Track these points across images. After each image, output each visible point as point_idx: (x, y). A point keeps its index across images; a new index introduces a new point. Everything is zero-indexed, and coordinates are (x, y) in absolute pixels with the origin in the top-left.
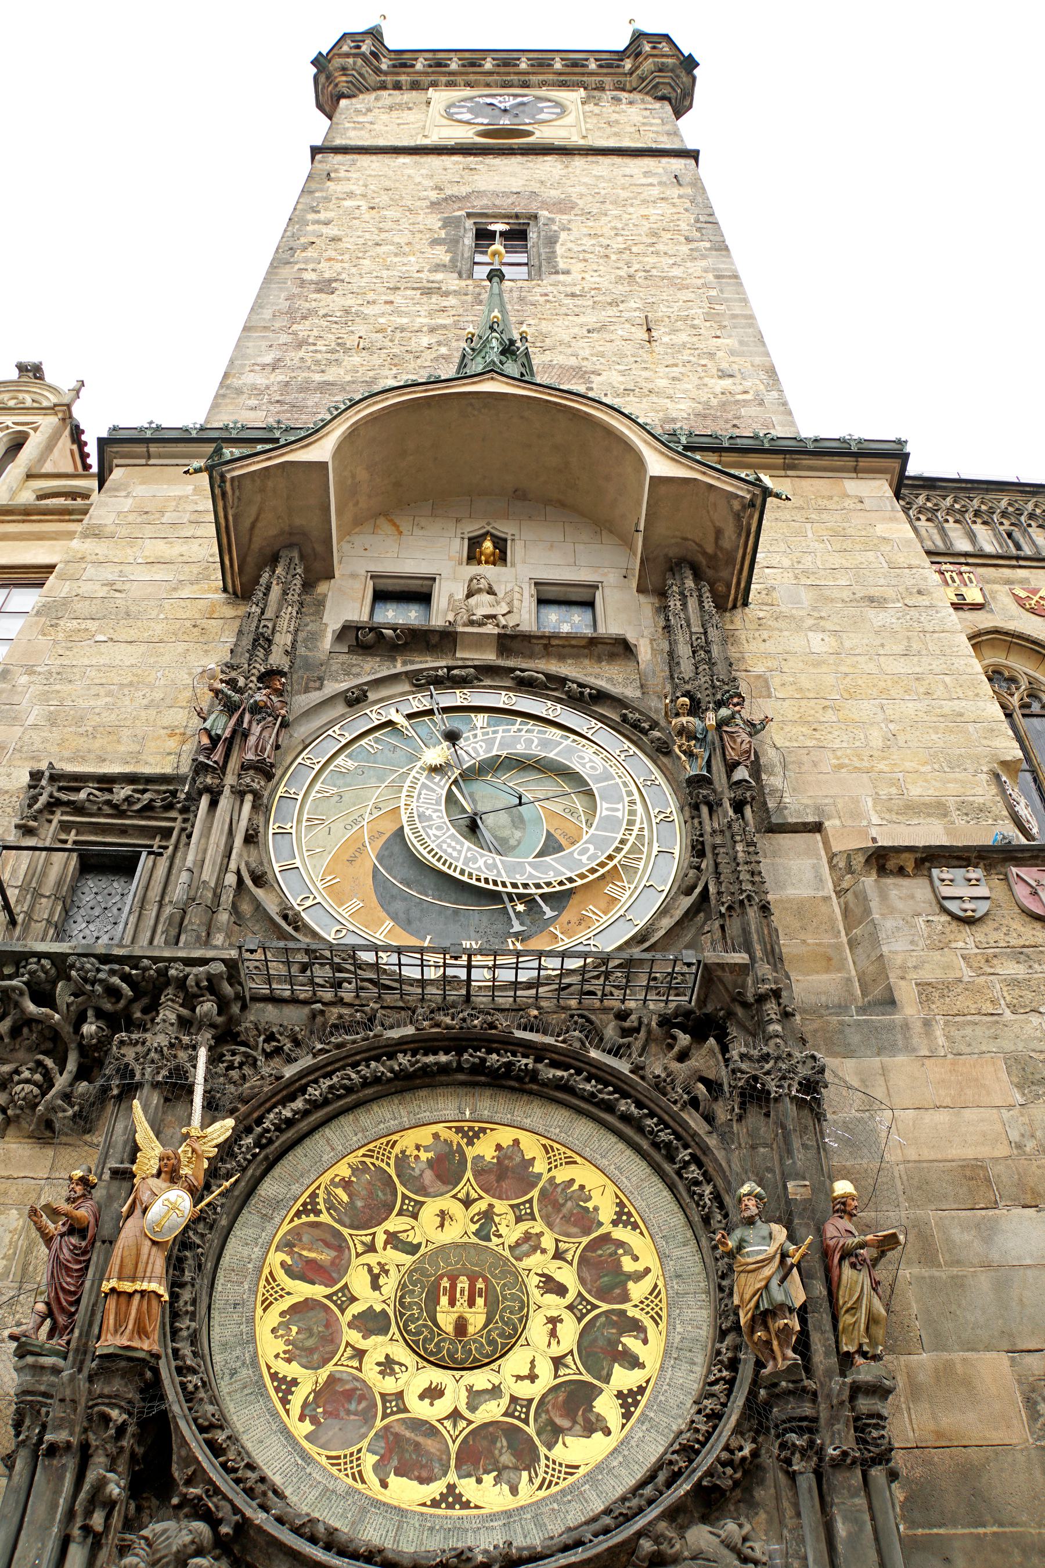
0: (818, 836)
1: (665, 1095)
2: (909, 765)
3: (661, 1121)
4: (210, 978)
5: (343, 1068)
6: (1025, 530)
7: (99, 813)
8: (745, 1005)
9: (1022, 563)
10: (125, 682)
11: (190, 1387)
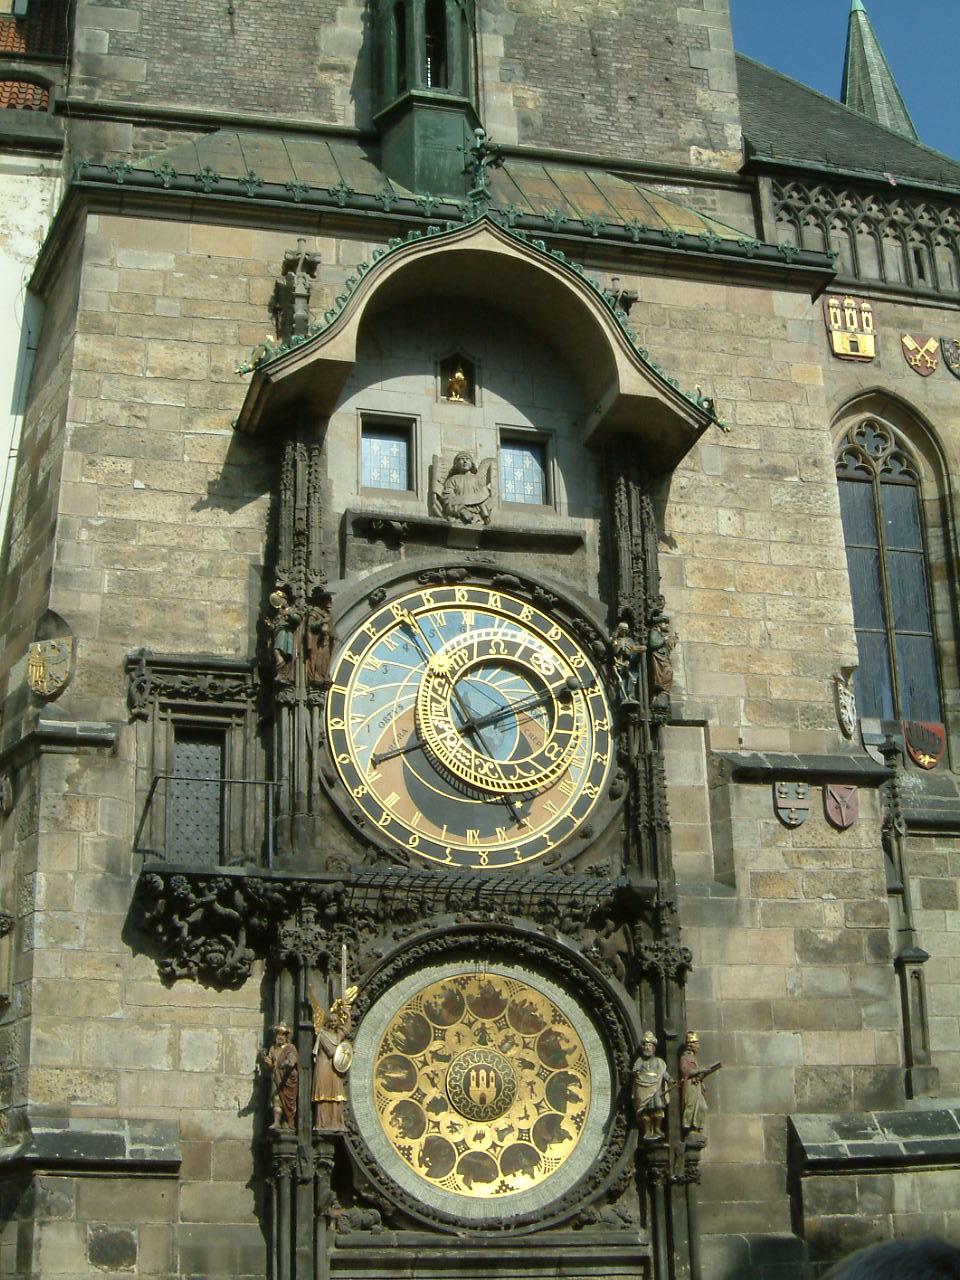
0: (702, 729)
2: (776, 667)
4: (335, 892)
6: (932, 255)
7: (186, 696)
8: (650, 908)
9: (920, 301)
10: (173, 543)
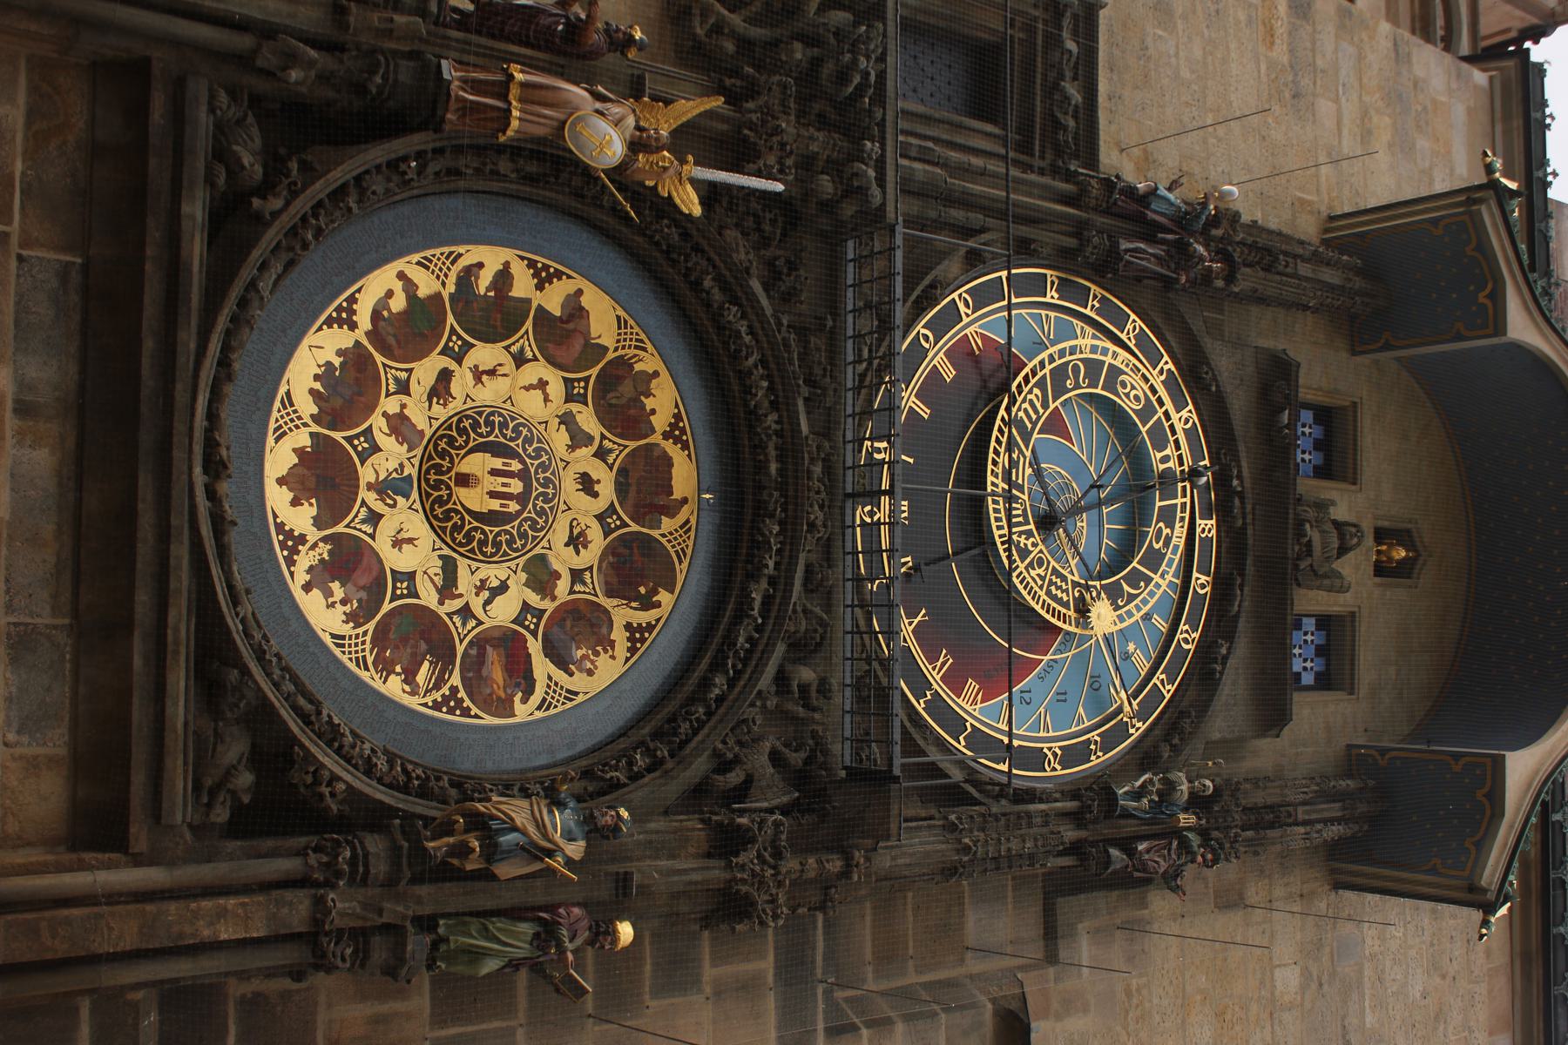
0: (1040, 955)
1: (732, 730)
3: (702, 724)
4: (862, 191)
5: (761, 349)
11: (403, 167)
